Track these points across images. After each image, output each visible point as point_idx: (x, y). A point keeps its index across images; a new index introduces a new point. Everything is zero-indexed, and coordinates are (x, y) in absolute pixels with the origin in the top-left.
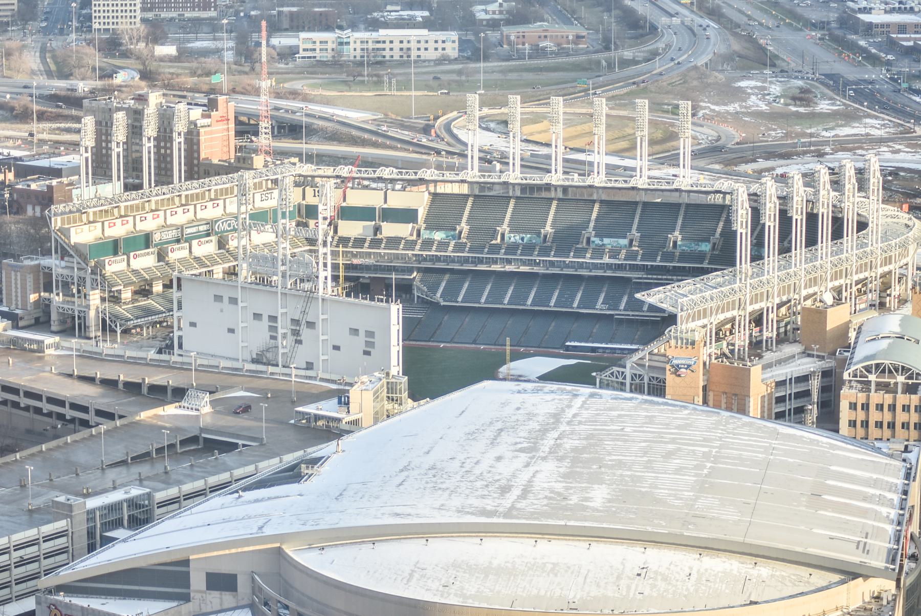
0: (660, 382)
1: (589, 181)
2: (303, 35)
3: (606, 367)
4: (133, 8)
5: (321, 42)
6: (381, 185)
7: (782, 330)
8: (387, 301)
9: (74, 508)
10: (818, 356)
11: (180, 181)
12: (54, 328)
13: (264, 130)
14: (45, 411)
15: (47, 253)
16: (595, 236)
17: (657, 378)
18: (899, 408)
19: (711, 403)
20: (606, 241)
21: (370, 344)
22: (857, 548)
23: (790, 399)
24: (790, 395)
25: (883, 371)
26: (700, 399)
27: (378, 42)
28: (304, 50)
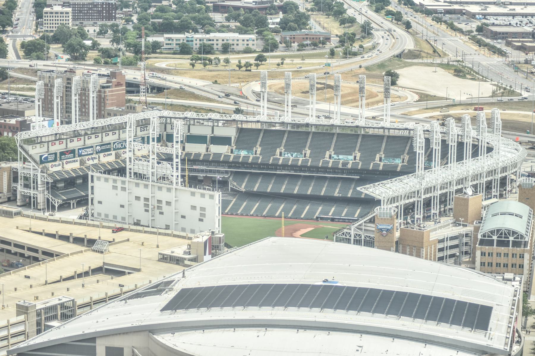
1: (331, 122)
2: (166, 36)
4: (67, 18)
5: (176, 40)
6: (210, 124)
7: (442, 209)
8: (213, 191)
9: (29, 308)
11: (93, 119)
13: (142, 90)
14: (13, 252)
16: (334, 154)
17: (369, 237)
18: (510, 256)
19: (401, 251)
20: (341, 157)
21: (201, 214)
22: (485, 336)
25: (501, 234)
26: (394, 249)
27: (210, 40)
28: (167, 44)
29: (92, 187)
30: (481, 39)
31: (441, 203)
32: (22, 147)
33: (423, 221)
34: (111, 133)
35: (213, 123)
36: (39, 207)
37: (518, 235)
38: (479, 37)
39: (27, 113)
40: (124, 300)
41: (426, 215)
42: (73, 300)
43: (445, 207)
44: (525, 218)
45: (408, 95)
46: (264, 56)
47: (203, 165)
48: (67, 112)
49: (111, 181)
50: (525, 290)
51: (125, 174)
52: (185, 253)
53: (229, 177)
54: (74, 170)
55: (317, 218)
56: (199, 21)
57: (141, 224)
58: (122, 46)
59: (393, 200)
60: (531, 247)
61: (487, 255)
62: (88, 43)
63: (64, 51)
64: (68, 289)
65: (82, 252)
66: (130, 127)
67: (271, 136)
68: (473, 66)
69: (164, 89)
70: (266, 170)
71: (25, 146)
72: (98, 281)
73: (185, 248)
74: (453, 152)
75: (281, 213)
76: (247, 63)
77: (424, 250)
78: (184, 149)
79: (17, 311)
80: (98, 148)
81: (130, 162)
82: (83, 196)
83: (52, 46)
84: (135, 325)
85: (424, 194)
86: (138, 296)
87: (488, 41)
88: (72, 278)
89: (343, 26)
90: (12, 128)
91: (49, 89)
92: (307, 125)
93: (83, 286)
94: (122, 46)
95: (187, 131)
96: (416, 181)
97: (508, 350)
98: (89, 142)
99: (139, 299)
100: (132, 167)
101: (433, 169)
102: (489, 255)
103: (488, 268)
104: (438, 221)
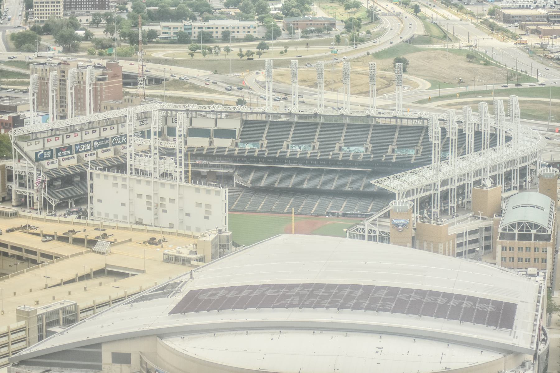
0: (386, 234)
1: (340, 112)
2: (163, 24)
3: (353, 226)
4: (58, 8)
5: (174, 28)
6: (214, 116)
7: (460, 202)
10: (482, 218)
11: (90, 113)
12: (14, 204)
15: (9, 158)
16: (345, 146)
17: (384, 232)
19: (418, 246)
20: (351, 149)
22: (510, 335)
23: (466, 244)
24: (466, 242)
27: (209, 28)
28: (163, 33)
29: (91, 185)
30: (493, 23)
31: (458, 195)
32: (16, 144)
33: (440, 214)
34: (108, 128)
35: (216, 116)
36: (35, 207)
37: (541, 228)
38: (491, 20)
39: (19, 109)
40: (129, 303)
41: (443, 209)
42: (75, 305)
43: (462, 200)
44: (547, 210)
45: (419, 83)
46: (266, 44)
47: (206, 160)
48: (61, 106)
49: (111, 179)
50: (549, 285)
51: (126, 170)
52: (191, 252)
53: (234, 172)
54: (71, 168)
55: (328, 214)
56: (197, 8)
57: (144, 223)
58: (116, 35)
59: (408, 194)
60: (553, 240)
61: (508, 249)
62: (81, 33)
63: (56, 42)
64: (70, 293)
65: (82, 253)
66: (131, 121)
67: (277, 127)
68: (486, 51)
69: (163, 80)
70: (272, 163)
71: (20, 143)
72: (100, 284)
73: (191, 247)
74: (470, 142)
75: (290, 208)
76: (248, 51)
77: (442, 245)
78: (186, 143)
79: (17, 316)
80: (96, 143)
81: (131, 158)
82: (82, 195)
83: (44, 38)
84: (142, 330)
85: (441, 186)
86: (143, 298)
87: (501, 24)
88: (73, 281)
89: (348, 11)
90: (4, 124)
91: (43, 81)
92: (316, 115)
93: (85, 289)
94: (116, 35)
95: (189, 124)
96: (432, 173)
97: (535, 349)
98: (86, 138)
99: (145, 302)
100: (132, 163)
101: (450, 160)
102: (510, 250)
103: (509, 263)
104: (455, 214)
